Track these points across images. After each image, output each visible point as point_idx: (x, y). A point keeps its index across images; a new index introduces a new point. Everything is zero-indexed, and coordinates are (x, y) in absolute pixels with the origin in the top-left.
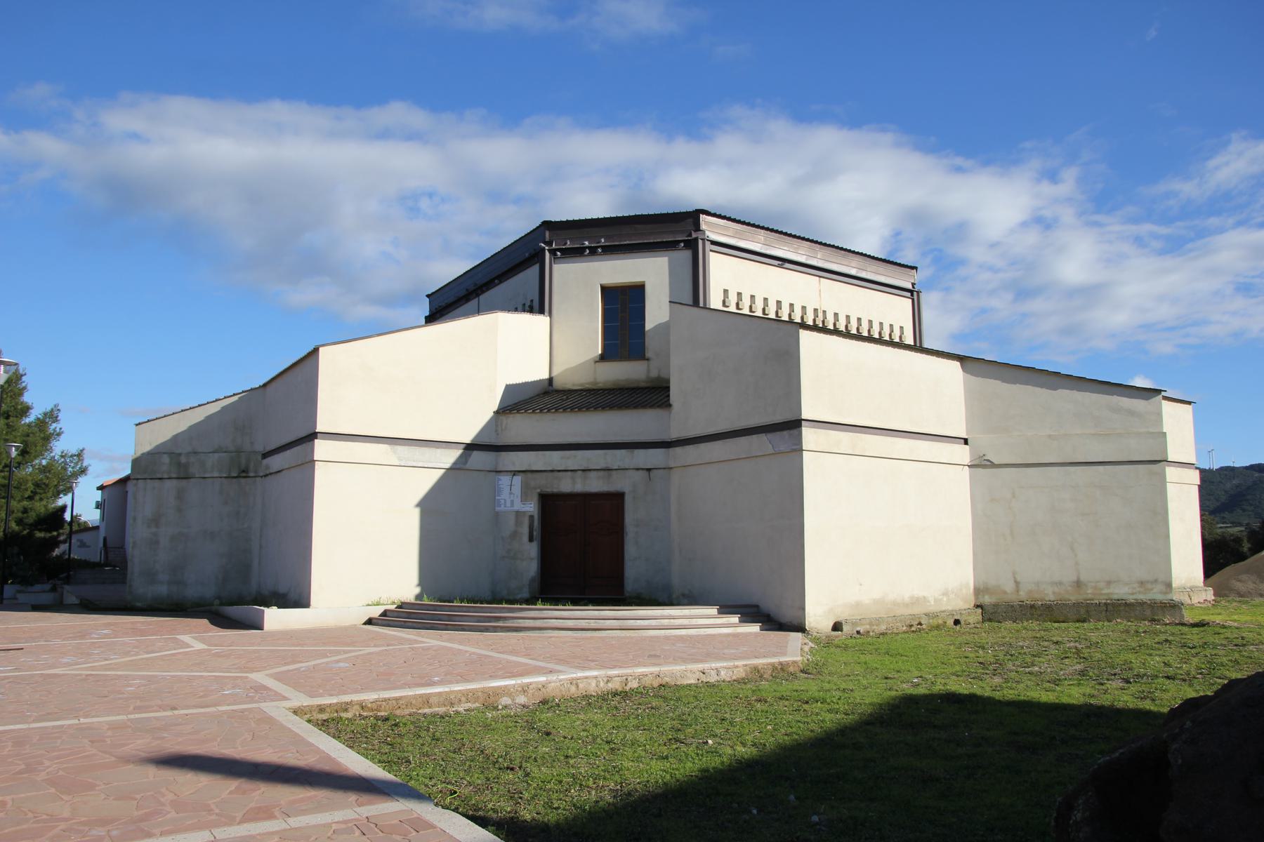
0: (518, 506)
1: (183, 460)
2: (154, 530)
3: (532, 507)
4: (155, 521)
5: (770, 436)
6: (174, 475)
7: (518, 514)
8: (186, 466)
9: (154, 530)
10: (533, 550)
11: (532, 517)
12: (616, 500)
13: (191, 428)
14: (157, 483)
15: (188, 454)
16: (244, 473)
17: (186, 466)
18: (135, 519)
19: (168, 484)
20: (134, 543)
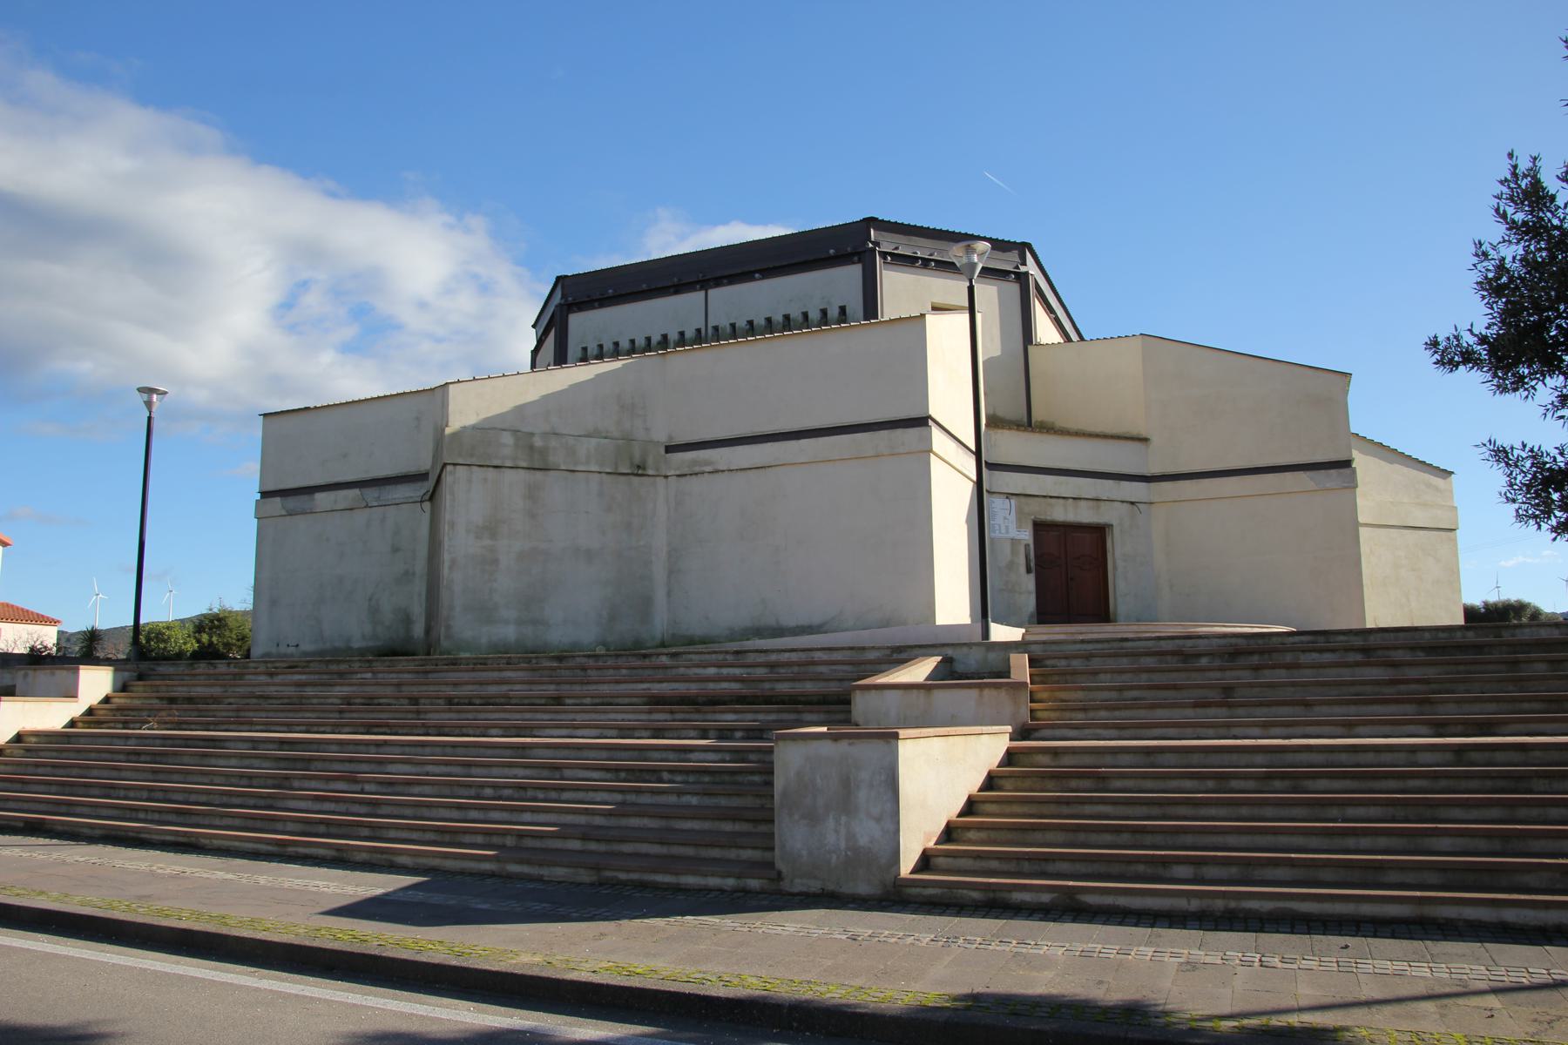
0: (1014, 533)
1: (538, 442)
2: (487, 542)
3: (1027, 535)
4: (491, 529)
5: (1309, 473)
6: (524, 464)
7: (1014, 542)
8: (543, 452)
9: (487, 542)
10: (1029, 582)
11: (1027, 546)
12: (1099, 533)
13: (546, 398)
14: (491, 473)
15: (545, 435)
16: (639, 470)
17: (543, 452)
18: (452, 525)
19: (510, 476)
20: (453, 562)
